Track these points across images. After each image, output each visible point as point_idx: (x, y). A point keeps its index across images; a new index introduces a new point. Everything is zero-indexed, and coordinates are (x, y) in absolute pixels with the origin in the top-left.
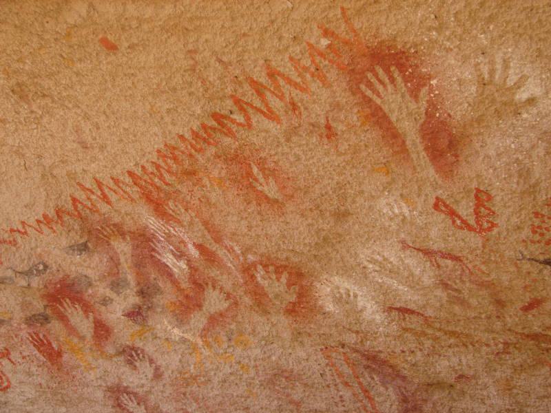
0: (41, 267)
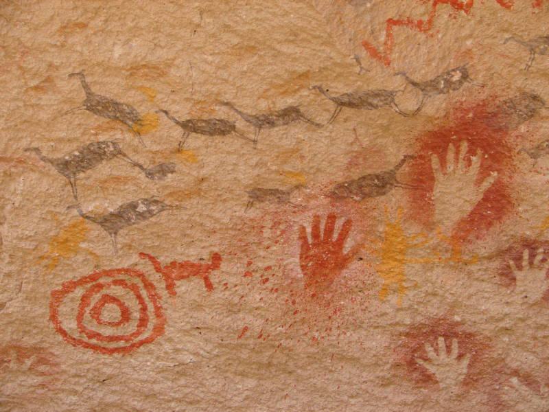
0: (457, 76)
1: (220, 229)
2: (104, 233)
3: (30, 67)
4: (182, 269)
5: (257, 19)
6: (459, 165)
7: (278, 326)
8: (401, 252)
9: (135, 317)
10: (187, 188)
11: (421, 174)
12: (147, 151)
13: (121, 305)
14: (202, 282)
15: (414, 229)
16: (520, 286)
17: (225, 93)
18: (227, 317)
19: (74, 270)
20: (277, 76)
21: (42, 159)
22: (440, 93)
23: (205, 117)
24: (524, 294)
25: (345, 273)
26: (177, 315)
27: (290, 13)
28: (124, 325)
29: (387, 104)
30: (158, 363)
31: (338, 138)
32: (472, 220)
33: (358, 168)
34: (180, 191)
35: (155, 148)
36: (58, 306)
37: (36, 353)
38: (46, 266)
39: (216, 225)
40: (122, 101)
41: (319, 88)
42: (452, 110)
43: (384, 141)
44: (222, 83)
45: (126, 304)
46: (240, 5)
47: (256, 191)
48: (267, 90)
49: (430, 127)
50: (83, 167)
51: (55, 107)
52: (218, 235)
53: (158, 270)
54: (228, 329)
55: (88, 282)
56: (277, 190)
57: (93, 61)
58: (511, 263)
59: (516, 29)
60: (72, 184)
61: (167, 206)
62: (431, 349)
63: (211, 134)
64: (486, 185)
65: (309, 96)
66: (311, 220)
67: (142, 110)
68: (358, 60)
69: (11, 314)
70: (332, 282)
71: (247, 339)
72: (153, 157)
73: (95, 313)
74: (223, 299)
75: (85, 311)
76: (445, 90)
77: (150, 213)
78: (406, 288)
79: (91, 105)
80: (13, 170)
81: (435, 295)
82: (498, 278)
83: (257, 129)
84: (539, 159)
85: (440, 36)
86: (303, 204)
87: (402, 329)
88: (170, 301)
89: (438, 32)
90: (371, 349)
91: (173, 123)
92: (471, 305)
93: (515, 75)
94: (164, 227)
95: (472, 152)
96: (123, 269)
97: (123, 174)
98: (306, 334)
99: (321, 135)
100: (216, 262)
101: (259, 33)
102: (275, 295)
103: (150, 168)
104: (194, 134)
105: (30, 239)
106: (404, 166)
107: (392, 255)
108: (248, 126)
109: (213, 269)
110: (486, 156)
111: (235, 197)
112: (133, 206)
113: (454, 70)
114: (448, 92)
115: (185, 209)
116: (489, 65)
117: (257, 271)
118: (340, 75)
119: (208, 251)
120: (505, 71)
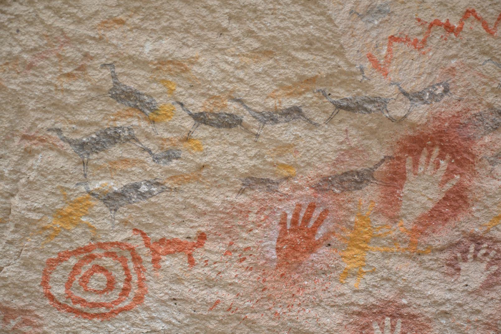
0: (440, 90)
1: (210, 212)
2: (105, 209)
3: (68, 55)
4: (169, 246)
5: (279, 28)
6: (429, 168)
7: (247, 300)
8: (366, 241)
9: (119, 286)
10: (188, 173)
11: (395, 173)
12: (158, 138)
13: (109, 275)
14: (186, 259)
15: (382, 220)
16: (463, 276)
17: (239, 91)
18: (203, 290)
19: (72, 241)
20: (288, 79)
21: (62, 139)
22: (425, 103)
23: (216, 111)
24: (465, 283)
25: (313, 256)
26: (156, 286)
27: (311, 24)
28: (108, 293)
29: (380, 110)
30: (132, 329)
31: (331, 137)
32: (432, 216)
33: (344, 165)
34: (181, 176)
35: (166, 135)
36: (50, 273)
37: (22, 314)
38: (46, 236)
39: (207, 208)
40: (144, 92)
41: (322, 92)
42: (432, 119)
43: (370, 142)
44: (237, 82)
45: (113, 275)
46: (267, 14)
47: (249, 180)
48: (277, 90)
49: (410, 133)
50: (97, 149)
51: (83, 93)
52: (208, 218)
53: (147, 245)
54: (202, 300)
55: (82, 253)
56: (268, 180)
57: (125, 54)
58: (459, 255)
59: (496, 53)
60: (84, 164)
61: (167, 187)
62: (378, 327)
63: (219, 126)
64: (448, 186)
65: (312, 98)
66: (294, 208)
67: (159, 101)
68: (362, 70)
69: (7, 278)
70: (300, 264)
71: (217, 311)
72: (162, 144)
73: (83, 281)
74: (202, 274)
75: (75, 279)
76: (429, 101)
77: (150, 194)
78: (365, 273)
79: (117, 94)
80: (34, 147)
81: (388, 280)
82: (445, 267)
83: (262, 124)
84: (496, 167)
85: (431, 54)
86: (289, 194)
87: (356, 309)
88: (153, 273)
89: (430, 50)
90: (325, 325)
91: (186, 114)
92: (419, 290)
93: (487, 92)
94: (160, 207)
95: (441, 156)
96: (117, 243)
97: (133, 157)
98: (269, 309)
99: (316, 133)
100: (201, 241)
101: (279, 40)
102: (249, 273)
103: (157, 153)
104: (204, 126)
105: (38, 211)
106: (383, 165)
107: (357, 243)
108: (254, 121)
109: (197, 247)
110: (453, 161)
111: (229, 184)
112: (136, 187)
113: (438, 85)
114: (431, 103)
115: (182, 191)
116: (468, 82)
117: (236, 251)
118: (343, 82)
119: (195, 230)
120: (480, 88)
